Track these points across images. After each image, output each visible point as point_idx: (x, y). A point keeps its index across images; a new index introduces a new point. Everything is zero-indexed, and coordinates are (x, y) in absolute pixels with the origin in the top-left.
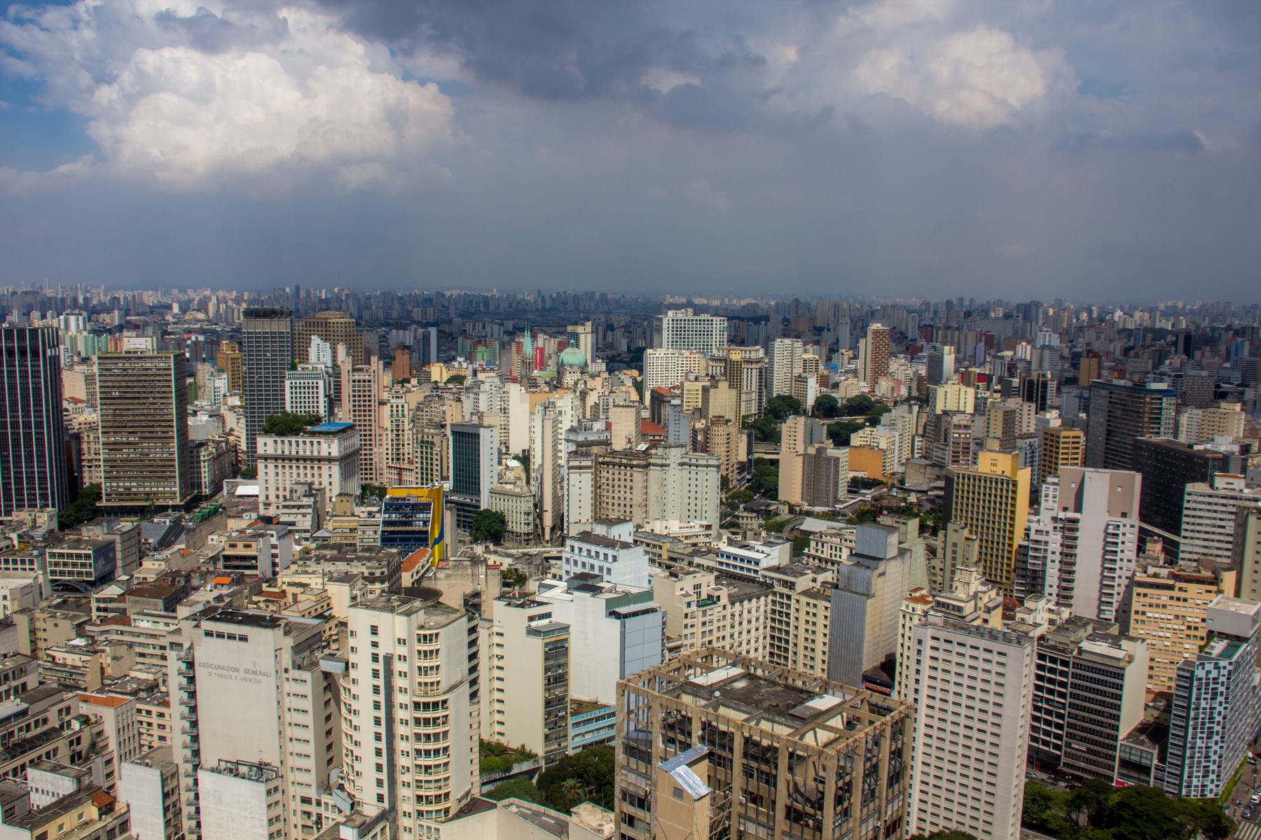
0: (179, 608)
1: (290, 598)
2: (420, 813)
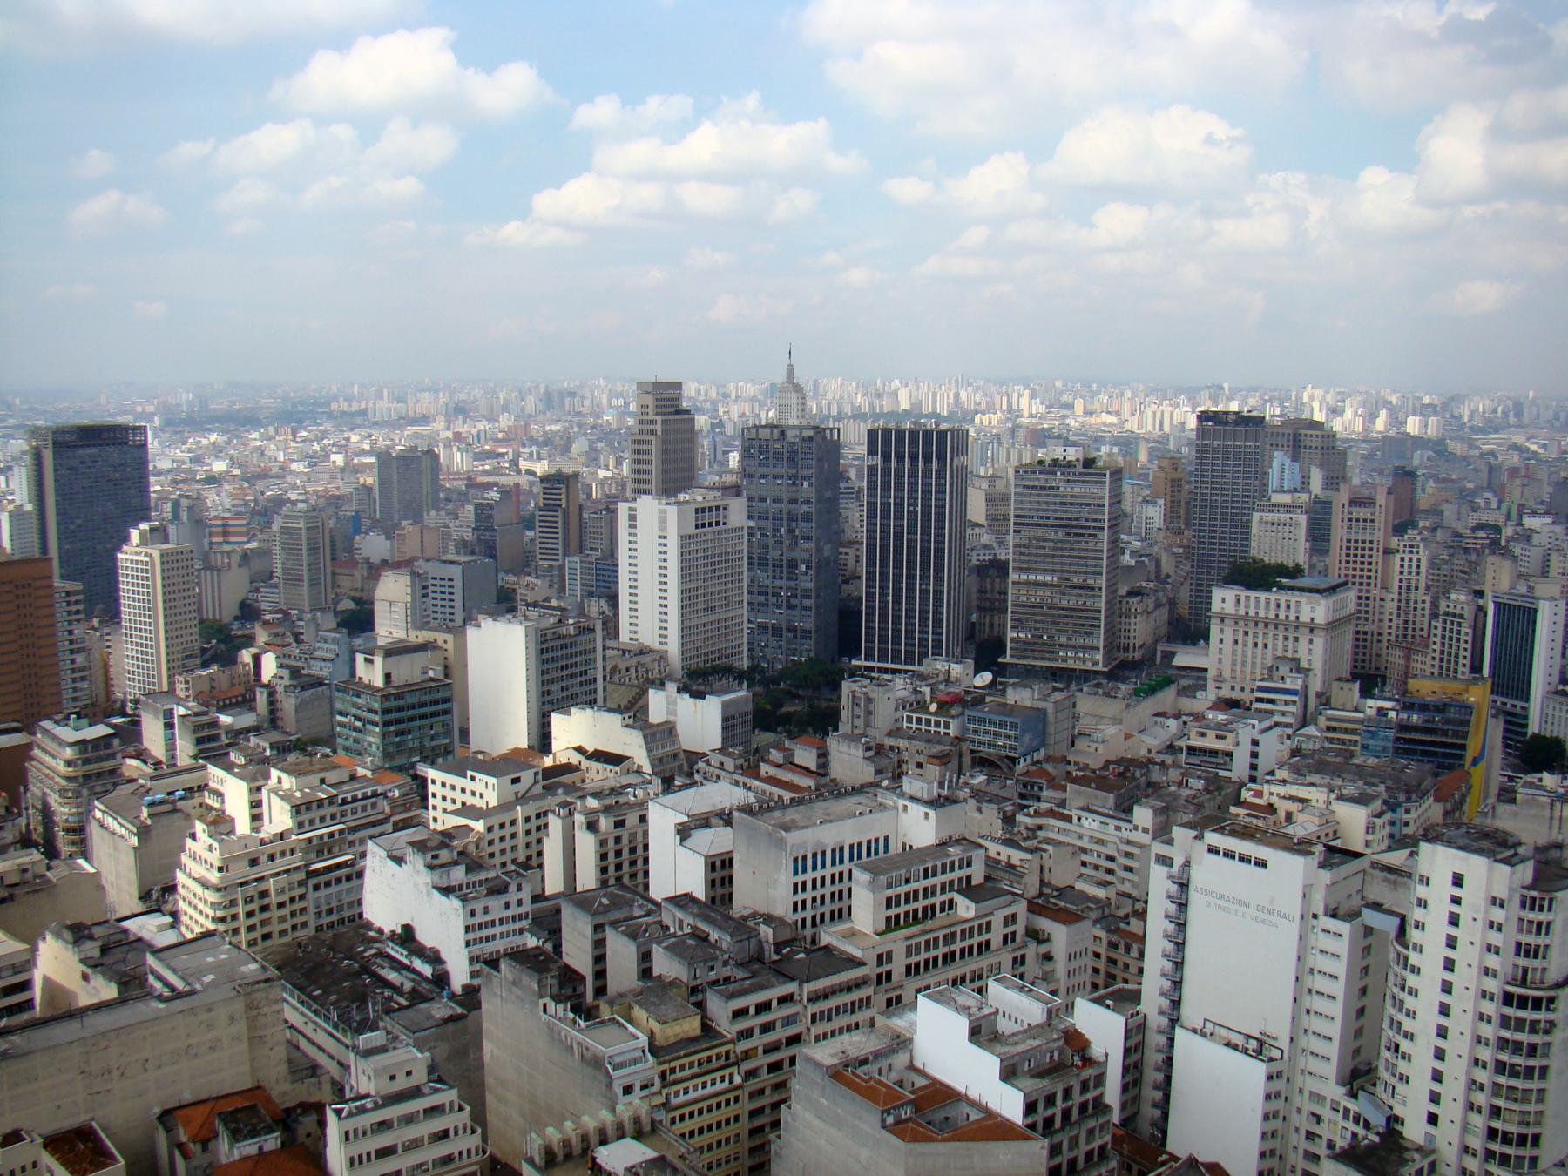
0: (1136, 809)
1: (1282, 815)
2: (1490, 1155)
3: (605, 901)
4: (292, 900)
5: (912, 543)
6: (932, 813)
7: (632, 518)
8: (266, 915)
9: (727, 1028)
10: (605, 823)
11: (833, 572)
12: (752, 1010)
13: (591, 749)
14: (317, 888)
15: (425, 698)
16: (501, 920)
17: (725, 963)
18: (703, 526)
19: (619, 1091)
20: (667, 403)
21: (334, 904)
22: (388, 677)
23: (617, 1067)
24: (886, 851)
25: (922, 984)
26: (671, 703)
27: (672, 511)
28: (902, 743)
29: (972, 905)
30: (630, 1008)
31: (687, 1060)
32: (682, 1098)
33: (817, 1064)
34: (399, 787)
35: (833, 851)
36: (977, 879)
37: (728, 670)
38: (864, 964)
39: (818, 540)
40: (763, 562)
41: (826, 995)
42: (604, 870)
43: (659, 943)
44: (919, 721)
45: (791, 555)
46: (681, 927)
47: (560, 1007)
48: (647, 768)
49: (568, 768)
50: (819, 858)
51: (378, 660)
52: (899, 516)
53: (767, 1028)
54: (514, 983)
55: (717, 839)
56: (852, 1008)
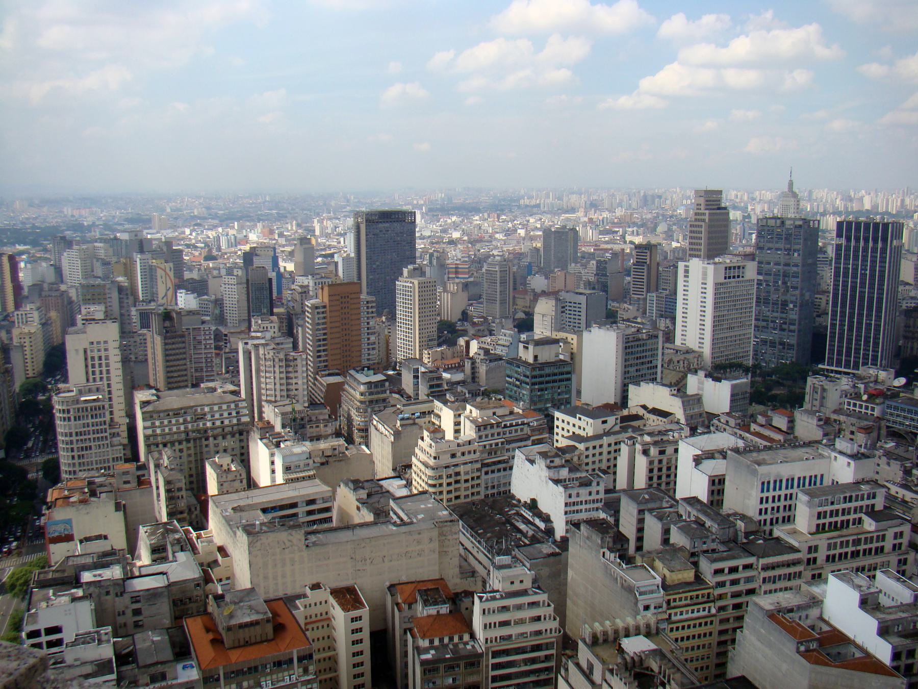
3: (647, 497)
4: (473, 479)
5: (862, 294)
6: (852, 463)
7: (687, 271)
8: (458, 486)
9: (711, 580)
10: (653, 451)
11: (810, 309)
12: (726, 571)
13: (650, 407)
14: (487, 473)
15: (556, 371)
16: (586, 501)
17: (713, 541)
18: (729, 278)
19: (641, 608)
20: (713, 205)
21: (496, 483)
22: (536, 357)
23: (641, 594)
24: (821, 484)
25: (835, 568)
26: (701, 383)
27: (711, 268)
28: (842, 418)
29: (874, 523)
30: (654, 560)
31: (683, 595)
32: (679, 617)
33: (761, 608)
34: (537, 420)
35: (787, 480)
36: (879, 507)
37: (739, 366)
38: (799, 551)
39: (802, 289)
40: (766, 302)
41: (773, 567)
42: (651, 479)
43: (675, 524)
44: (855, 405)
45: (784, 298)
46: (689, 517)
47: (612, 555)
48: (683, 421)
49: (637, 417)
50: (778, 484)
51: (531, 347)
52: (855, 276)
53: (734, 582)
54: (588, 538)
55: (716, 466)
56: (789, 577)
